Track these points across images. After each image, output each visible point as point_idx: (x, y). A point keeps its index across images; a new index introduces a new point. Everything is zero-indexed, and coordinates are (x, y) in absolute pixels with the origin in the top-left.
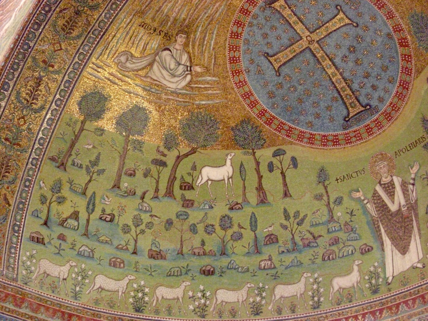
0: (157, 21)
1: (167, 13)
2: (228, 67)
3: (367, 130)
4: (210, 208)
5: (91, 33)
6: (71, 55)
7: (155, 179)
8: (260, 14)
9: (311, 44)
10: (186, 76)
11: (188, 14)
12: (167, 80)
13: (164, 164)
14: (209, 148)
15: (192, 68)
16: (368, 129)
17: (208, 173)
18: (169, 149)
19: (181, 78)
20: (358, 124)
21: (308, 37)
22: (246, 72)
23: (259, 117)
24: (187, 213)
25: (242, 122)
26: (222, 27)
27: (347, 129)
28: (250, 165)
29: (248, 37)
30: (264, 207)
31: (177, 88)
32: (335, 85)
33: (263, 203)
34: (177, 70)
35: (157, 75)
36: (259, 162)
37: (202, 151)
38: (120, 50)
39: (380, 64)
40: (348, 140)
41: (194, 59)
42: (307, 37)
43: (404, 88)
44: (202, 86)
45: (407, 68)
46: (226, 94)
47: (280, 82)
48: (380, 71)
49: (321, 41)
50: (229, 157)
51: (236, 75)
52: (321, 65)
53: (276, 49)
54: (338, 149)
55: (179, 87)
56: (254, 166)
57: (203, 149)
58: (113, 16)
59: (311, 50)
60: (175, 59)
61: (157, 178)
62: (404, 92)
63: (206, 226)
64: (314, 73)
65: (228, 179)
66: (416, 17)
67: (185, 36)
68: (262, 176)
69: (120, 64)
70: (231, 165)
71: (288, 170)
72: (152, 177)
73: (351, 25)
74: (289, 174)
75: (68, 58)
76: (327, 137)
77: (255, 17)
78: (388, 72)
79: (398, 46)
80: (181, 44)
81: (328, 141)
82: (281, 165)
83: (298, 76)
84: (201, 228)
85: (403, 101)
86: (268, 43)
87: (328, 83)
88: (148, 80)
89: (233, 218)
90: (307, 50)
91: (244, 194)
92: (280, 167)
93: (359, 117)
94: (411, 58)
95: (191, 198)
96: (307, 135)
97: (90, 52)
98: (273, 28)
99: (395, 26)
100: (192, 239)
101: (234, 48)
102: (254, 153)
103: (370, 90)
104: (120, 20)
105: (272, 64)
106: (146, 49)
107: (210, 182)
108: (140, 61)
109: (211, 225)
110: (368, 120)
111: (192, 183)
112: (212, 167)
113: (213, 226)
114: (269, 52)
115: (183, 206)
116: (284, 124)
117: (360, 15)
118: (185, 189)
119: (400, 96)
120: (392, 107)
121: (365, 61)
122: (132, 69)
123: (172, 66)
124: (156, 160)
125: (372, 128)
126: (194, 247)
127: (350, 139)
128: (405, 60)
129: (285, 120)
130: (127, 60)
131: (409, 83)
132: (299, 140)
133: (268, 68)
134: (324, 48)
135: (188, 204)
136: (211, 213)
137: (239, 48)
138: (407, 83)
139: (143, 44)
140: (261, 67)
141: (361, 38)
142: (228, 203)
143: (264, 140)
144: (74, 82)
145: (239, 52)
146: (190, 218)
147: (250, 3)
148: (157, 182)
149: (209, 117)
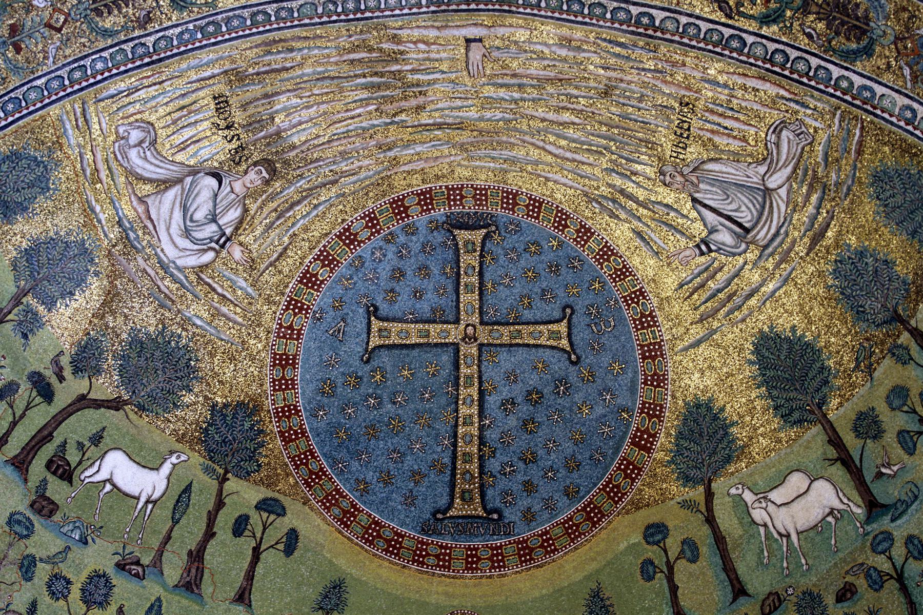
0: (248, 114)
1: (277, 112)
2: (291, 285)
3: (468, 556)
4: (80, 540)
5: (131, 44)
6: (65, 57)
7: (14, 414)
8: (423, 230)
9: (466, 343)
10: (205, 251)
11: (306, 142)
12: (169, 234)
13: (47, 394)
14: (147, 416)
15: (228, 244)
16: (472, 556)
17: (115, 467)
18: (77, 370)
19: (196, 247)
20: (457, 537)
21: (470, 328)
22: (314, 317)
23: (278, 416)
24: (33, 525)
25: (241, 404)
26: (341, 207)
27: (429, 536)
28: (202, 502)
29: (367, 255)
30: (187, 598)
31: (174, 263)
32: (456, 441)
33: (187, 589)
34: (203, 227)
35: (162, 211)
36: (225, 504)
37: (132, 416)
38: (146, 116)
39: (569, 451)
40: (420, 556)
41: (245, 229)
42: (468, 325)
43: (589, 519)
44: (220, 290)
45: (618, 486)
46: (249, 334)
47: (360, 374)
48: (559, 464)
49: (487, 349)
50: (174, 459)
51: (293, 310)
52: (457, 390)
53: (396, 310)
54: (391, 562)
55: (179, 262)
56: (210, 506)
57: (136, 413)
58: (193, 44)
59: (458, 352)
60: (215, 205)
61: (17, 415)
62: (584, 527)
63: (55, 576)
64: (432, 397)
65: (147, 502)
66: (703, 410)
67: (267, 176)
68: (214, 534)
69: (122, 142)
70: (168, 479)
71: (271, 549)
72: (12, 407)
73: (566, 355)
74: (270, 558)
75: (54, 58)
76: (381, 528)
77: (411, 231)
78: (575, 475)
79: (628, 440)
80: (249, 185)
81: (379, 536)
82: (263, 533)
83: (400, 384)
84: (43, 572)
85: (572, 540)
86: (392, 291)
87: (444, 429)
88: (140, 210)
89: (115, 589)
90: (451, 349)
91: (160, 552)
92: (258, 535)
93: (466, 525)
94: (638, 474)
95: (56, 498)
96: (345, 504)
97: (99, 77)
98: (424, 270)
99: (650, 404)
100: (16, 587)
101: (326, 259)
102: (223, 480)
103: (516, 487)
104: (197, 61)
105: (369, 333)
106: (184, 149)
107: (108, 487)
108: (157, 162)
109: (65, 578)
110: (481, 539)
111: (75, 468)
112: (130, 458)
113: (69, 582)
114: (381, 308)
115: (32, 506)
116: (313, 457)
117: (598, 348)
118: (54, 473)
119: (572, 531)
120: (544, 541)
121: (543, 432)
122: (132, 167)
123: (199, 216)
124: (39, 374)
125: (479, 559)
126: (11, 607)
127: (424, 557)
128: (624, 471)
129: (321, 449)
130: (140, 144)
131: (603, 516)
132: (324, 504)
133: (359, 335)
134: (486, 363)
135: (43, 507)
136: (77, 552)
137: (335, 266)
138: (600, 512)
139: (191, 134)
140: (346, 325)
141: (566, 388)
142: (121, 551)
143: (259, 466)
144: (25, 112)
145: (331, 272)
146: (34, 538)
147: (420, 200)
148: (14, 424)
149: (187, 357)
